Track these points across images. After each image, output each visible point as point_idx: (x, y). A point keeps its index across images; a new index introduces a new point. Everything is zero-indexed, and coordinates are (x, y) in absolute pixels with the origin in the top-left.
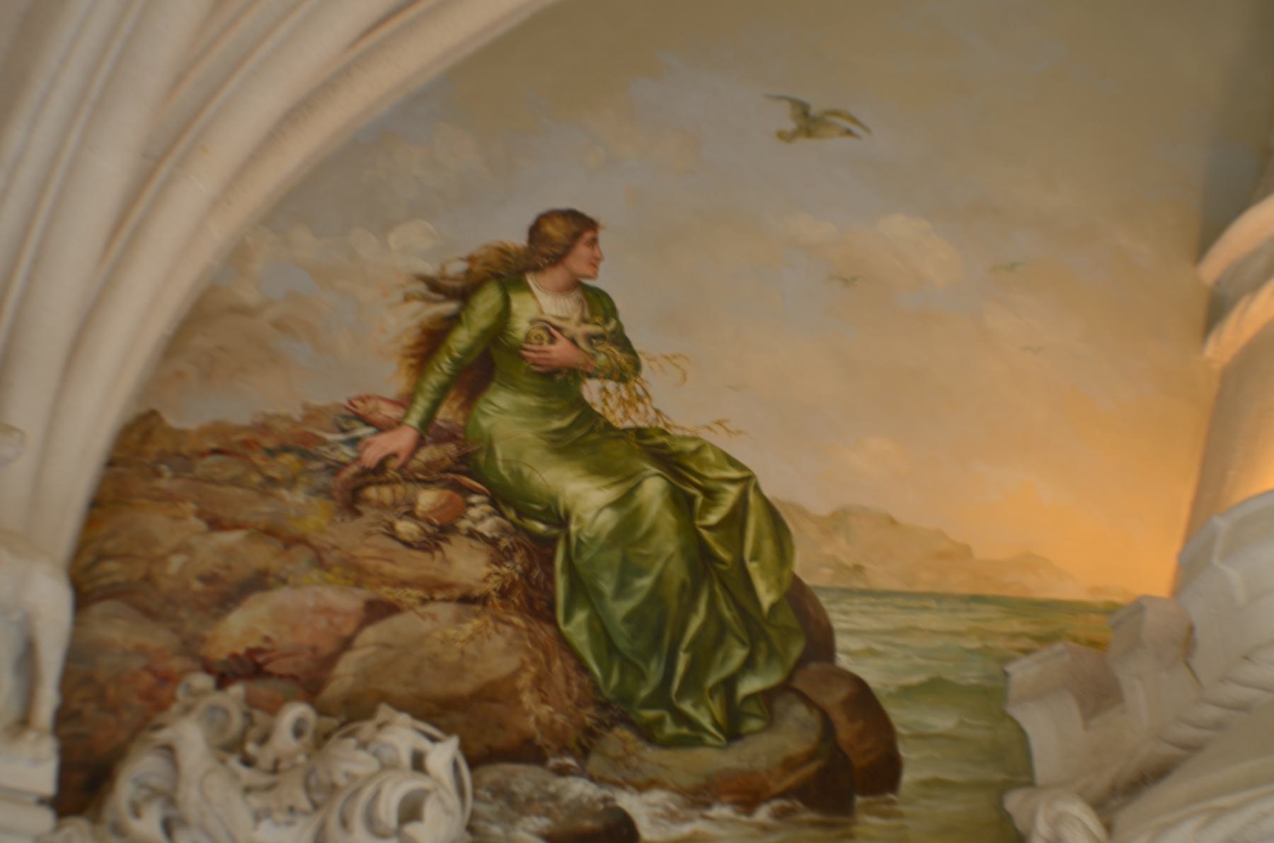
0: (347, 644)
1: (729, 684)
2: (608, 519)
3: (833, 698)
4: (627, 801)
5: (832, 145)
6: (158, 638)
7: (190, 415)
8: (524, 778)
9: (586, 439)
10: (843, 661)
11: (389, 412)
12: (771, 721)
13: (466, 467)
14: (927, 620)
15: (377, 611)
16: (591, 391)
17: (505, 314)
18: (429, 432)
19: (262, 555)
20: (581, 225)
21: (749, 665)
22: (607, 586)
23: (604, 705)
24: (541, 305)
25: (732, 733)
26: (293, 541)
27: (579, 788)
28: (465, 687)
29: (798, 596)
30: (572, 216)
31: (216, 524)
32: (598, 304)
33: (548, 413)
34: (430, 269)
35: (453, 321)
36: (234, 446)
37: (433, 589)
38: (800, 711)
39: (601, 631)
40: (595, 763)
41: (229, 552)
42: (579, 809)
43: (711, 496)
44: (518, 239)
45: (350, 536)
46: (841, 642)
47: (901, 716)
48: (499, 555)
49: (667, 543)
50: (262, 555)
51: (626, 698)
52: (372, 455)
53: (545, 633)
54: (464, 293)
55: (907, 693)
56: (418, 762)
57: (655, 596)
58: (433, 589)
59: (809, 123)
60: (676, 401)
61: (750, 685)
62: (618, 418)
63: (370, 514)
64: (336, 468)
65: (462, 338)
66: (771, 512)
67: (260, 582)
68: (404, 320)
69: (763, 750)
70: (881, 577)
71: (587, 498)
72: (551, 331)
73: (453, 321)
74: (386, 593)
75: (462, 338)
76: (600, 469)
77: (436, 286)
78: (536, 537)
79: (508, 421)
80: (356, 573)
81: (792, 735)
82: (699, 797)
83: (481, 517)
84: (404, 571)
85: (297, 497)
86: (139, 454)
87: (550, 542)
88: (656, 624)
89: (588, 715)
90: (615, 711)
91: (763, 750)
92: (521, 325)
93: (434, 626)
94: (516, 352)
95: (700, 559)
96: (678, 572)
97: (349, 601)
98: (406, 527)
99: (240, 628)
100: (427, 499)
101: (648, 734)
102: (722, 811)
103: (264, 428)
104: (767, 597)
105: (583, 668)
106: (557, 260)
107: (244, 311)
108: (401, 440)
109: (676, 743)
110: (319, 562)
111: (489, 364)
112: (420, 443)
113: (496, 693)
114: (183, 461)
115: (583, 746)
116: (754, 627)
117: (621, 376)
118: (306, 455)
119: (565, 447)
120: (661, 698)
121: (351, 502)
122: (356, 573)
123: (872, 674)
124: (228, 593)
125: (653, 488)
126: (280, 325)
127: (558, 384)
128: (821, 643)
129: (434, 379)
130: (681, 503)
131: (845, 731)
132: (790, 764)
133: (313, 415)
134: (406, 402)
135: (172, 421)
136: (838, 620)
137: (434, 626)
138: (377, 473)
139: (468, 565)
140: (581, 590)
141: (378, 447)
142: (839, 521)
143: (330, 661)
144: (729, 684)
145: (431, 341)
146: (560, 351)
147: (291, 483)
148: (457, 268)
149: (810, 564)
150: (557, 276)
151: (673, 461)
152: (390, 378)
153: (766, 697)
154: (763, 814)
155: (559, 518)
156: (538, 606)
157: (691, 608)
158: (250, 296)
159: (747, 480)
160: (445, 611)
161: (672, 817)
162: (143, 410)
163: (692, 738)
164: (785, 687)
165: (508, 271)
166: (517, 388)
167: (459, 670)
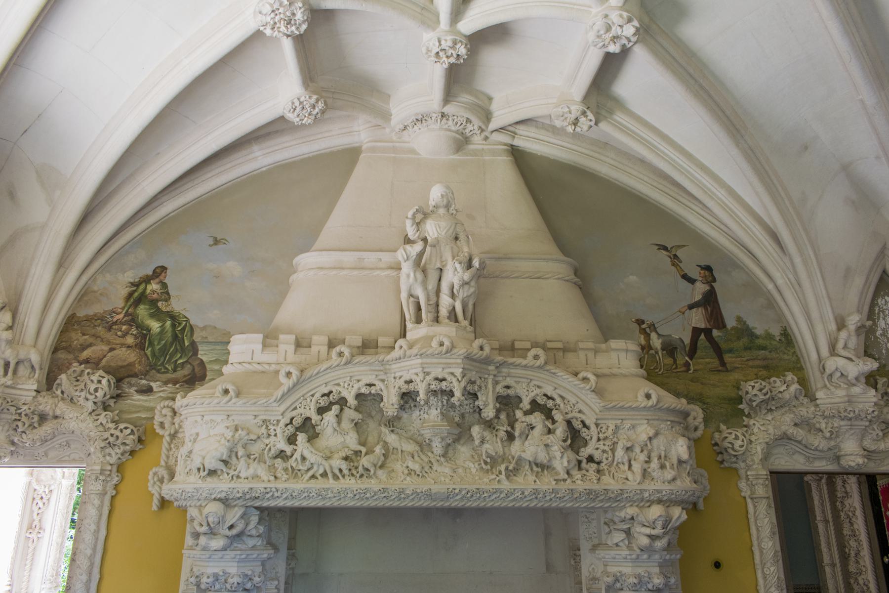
0: (105, 356)
1: (176, 361)
2: (158, 330)
3: (196, 363)
4: (152, 384)
5: (221, 246)
6: (71, 356)
7: (81, 313)
8: (134, 380)
9: (157, 314)
10: (199, 356)
11: (120, 311)
12: (183, 368)
13: (132, 320)
14: (218, 347)
15: (112, 350)
16: (160, 304)
17: (145, 289)
18: (127, 314)
19: (91, 340)
20: (164, 269)
21: (180, 358)
22: (156, 343)
23: (151, 366)
24: (154, 286)
25: (175, 370)
26: (97, 337)
27: (144, 382)
28: (125, 364)
29: (193, 344)
30: (162, 267)
31: (84, 335)
32: (164, 285)
33: (150, 309)
34: (132, 280)
35: (135, 291)
36: (88, 319)
37: (122, 345)
38: (189, 366)
39: (153, 352)
40: (147, 377)
41: (86, 340)
42: (143, 385)
43: (180, 324)
44: (150, 273)
45: (109, 336)
46: (200, 352)
47: (208, 366)
48: (136, 337)
49: (169, 334)
50: (91, 340)
51: (155, 364)
52: (115, 320)
53: (142, 353)
54: (137, 285)
55: (211, 362)
56: (99, 382)
57: (165, 345)
58: (122, 345)
59: (216, 242)
60: (176, 305)
61: (180, 361)
62: (164, 309)
63: (113, 331)
64: (108, 322)
65: (136, 294)
66: (191, 327)
67: (90, 345)
68: (124, 292)
69: (180, 373)
70: (210, 339)
71: (155, 326)
72: (154, 292)
73: (135, 291)
74: (114, 346)
75: (136, 294)
76: (158, 320)
77: (132, 284)
78: (144, 335)
79: (142, 311)
80: (109, 343)
81: (187, 371)
82: (166, 383)
83: (134, 331)
84: (118, 342)
85: (100, 328)
86: (70, 322)
87: (145, 335)
88: (164, 351)
89: (148, 368)
90: (152, 367)
91: (180, 373)
92: (148, 291)
93: (122, 352)
94: (146, 297)
95: (175, 337)
96: (170, 339)
97: (106, 348)
98: (119, 333)
99: (85, 354)
100: (124, 327)
101: (159, 371)
102: (170, 385)
103: (95, 315)
104: (187, 344)
105: (148, 359)
106: (157, 277)
107: (95, 292)
108: (121, 316)
109: (164, 373)
110: (102, 341)
111: (142, 299)
112: (125, 316)
113: (131, 364)
114: (79, 323)
115: (145, 374)
116: (183, 350)
117: (166, 301)
118: (102, 320)
119: (152, 316)
120: (162, 364)
121: (110, 329)
122: (109, 343)
123: (204, 359)
124: (84, 348)
125: (169, 323)
126: (101, 294)
127: (153, 303)
128: (196, 353)
129: (129, 303)
130: (173, 326)
131: (197, 369)
132: (185, 376)
133: (105, 312)
134: (123, 309)
135: (78, 315)
136: (200, 348)
137: (122, 352)
138: (115, 323)
139: (130, 340)
140: (151, 344)
141: (117, 317)
142: (204, 328)
143: (101, 359)
144: (176, 361)
145: (130, 295)
146: (155, 296)
147: (99, 326)
148: (137, 280)
149: (197, 337)
150: (157, 280)
151: (173, 317)
152: (120, 303)
153: (183, 363)
154: (177, 386)
155: (149, 330)
156: (142, 348)
157: (171, 347)
158: (96, 288)
159: (188, 321)
160: (124, 349)
161: (160, 387)
162: (70, 313)
163: (167, 371)
164: (187, 362)
165: (147, 280)
166: (145, 304)
167: (125, 360)
